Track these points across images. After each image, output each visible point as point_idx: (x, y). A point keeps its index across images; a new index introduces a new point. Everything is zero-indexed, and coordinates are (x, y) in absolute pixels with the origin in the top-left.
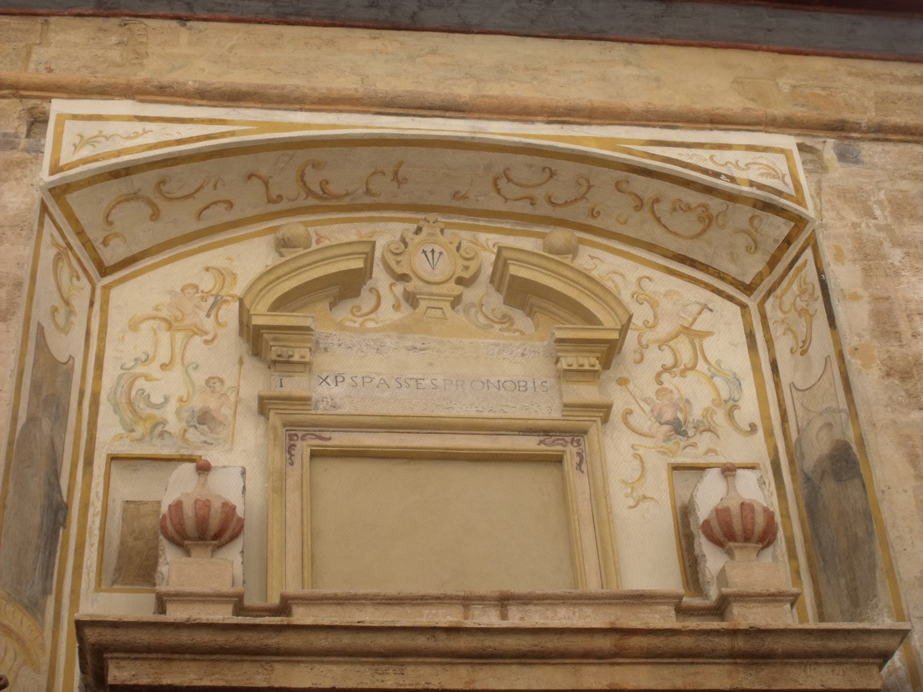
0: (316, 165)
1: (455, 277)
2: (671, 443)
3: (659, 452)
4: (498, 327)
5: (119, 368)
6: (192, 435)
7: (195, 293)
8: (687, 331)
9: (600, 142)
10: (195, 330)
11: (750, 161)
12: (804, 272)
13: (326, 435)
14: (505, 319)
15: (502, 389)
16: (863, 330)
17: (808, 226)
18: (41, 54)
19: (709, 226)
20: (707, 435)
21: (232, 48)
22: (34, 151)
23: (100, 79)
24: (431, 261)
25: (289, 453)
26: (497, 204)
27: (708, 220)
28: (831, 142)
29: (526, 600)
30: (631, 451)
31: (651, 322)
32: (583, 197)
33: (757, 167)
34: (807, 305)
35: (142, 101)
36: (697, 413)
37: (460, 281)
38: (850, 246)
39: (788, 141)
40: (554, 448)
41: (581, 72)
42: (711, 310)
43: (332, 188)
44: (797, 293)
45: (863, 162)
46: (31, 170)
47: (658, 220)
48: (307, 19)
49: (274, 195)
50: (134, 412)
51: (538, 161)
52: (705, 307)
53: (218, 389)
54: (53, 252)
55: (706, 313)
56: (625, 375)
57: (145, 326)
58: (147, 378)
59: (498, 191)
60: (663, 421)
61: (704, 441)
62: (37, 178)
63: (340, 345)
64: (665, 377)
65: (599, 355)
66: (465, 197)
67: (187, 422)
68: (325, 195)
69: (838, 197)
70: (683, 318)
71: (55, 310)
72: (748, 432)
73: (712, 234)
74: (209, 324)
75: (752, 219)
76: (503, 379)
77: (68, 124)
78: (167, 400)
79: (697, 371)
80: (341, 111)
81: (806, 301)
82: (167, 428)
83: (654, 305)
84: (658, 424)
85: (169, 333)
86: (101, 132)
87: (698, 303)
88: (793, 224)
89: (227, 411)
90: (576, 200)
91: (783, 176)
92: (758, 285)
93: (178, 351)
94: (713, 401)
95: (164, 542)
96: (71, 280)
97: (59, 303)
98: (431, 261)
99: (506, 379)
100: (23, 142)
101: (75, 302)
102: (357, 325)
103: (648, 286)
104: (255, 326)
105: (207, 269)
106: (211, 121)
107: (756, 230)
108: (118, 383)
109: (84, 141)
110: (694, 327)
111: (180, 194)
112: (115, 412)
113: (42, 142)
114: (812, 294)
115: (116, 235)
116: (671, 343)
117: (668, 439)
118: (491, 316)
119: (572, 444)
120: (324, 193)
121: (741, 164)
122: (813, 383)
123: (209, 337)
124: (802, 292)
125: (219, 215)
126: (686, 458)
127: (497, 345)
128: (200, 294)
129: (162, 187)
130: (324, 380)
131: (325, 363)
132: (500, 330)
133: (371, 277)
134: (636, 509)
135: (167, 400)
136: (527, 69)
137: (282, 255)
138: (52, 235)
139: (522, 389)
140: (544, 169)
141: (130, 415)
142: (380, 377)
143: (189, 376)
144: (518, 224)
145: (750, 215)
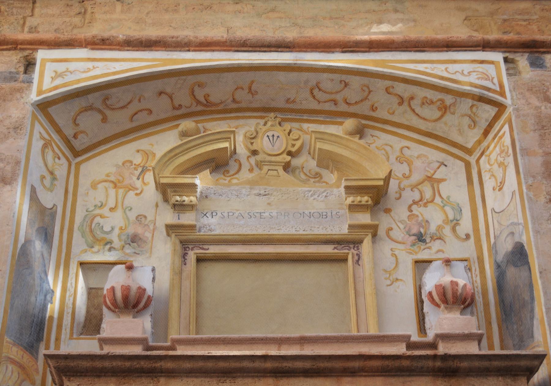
0: (201, 85)
1: (286, 151)
2: (415, 247)
3: (408, 252)
4: (312, 180)
5: (85, 211)
6: (128, 250)
7: (130, 166)
8: (429, 178)
10: (130, 187)
11: (472, 70)
12: (503, 139)
13: (206, 247)
14: (318, 176)
15: (312, 217)
16: (537, 173)
17: (507, 110)
19: (445, 112)
20: (438, 241)
21: (148, 13)
22: (28, 82)
23: (65, 36)
24: (272, 142)
25: (184, 258)
26: (314, 105)
27: (444, 109)
28: (526, 55)
30: (391, 252)
31: (407, 174)
32: (366, 98)
33: (475, 74)
34: (504, 160)
35: (93, 49)
36: (433, 228)
37: (290, 153)
38: (533, 121)
39: (498, 57)
40: (342, 251)
41: (366, 18)
42: (446, 166)
43: (212, 99)
44: (499, 152)
45: (546, 67)
46: (26, 94)
47: (413, 111)
49: (176, 104)
50: (94, 236)
52: (443, 164)
53: (143, 222)
54: (41, 143)
55: (443, 167)
56: (389, 207)
57: (100, 186)
58: (101, 216)
59: (314, 97)
60: (411, 233)
61: (436, 245)
62: (30, 99)
63: (215, 194)
64: (414, 207)
65: (371, 195)
66: (294, 102)
67: (125, 242)
68: (208, 104)
69: (528, 90)
70: (428, 171)
71: (43, 177)
72: (464, 239)
73: (448, 117)
74: (138, 184)
75: (472, 106)
76: (312, 211)
77: (48, 65)
78: (113, 229)
79: (435, 203)
81: (503, 157)
82: (113, 245)
83: (410, 164)
84: (408, 236)
85: (115, 190)
86: (68, 69)
87: (438, 162)
88: (497, 109)
89: (148, 235)
90: (362, 101)
91: (493, 78)
92: (475, 149)
93: (120, 200)
94: (444, 221)
95: (105, 310)
96: (54, 160)
98: (272, 142)
99: (315, 211)
100: (22, 76)
101: (57, 173)
102: (227, 182)
104: (162, 184)
105: (138, 151)
107: (474, 114)
108: (84, 220)
109: (58, 75)
110: (434, 177)
112: (83, 237)
113: (33, 77)
114: (507, 153)
115: (82, 132)
116: (419, 187)
117: (413, 245)
118: (308, 174)
119: (354, 249)
120: (207, 102)
121: (466, 72)
122: (505, 207)
123: (138, 192)
124: (502, 152)
125: (143, 118)
126: (423, 255)
127: (310, 191)
128: (134, 166)
129: (108, 103)
130: (205, 215)
132: (314, 182)
133: (236, 153)
134: (391, 286)
135: (113, 229)
136: (331, 18)
137: (182, 140)
138: (40, 133)
139: (324, 217)
141: (92, 239)
142: (238, 212)
143: (126, 214)
144: (327, 118)
145: (470, 105)
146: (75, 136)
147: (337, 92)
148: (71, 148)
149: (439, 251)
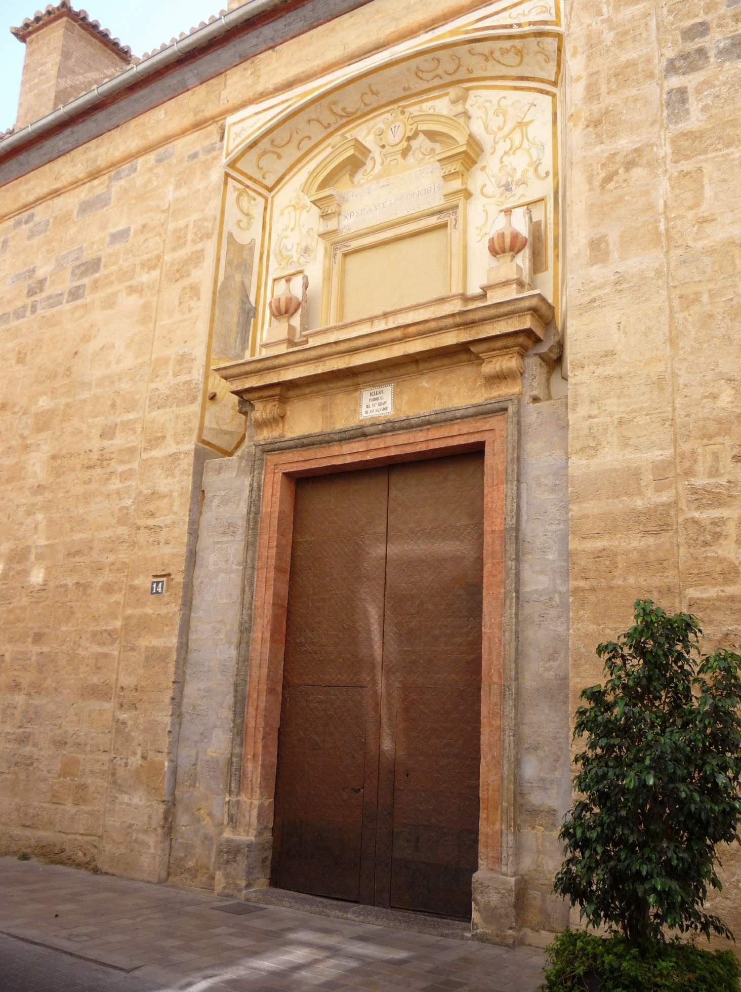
0: (335, 103)
9: (452, 33)
13: (349, 244)
18: (224, 94)
19: (522, 56)
26: (426, 86)
29: (395, 313)
36: (518, 175)
43: (349, 110)
47: (499, 62)
48: (321, 21)
51: (426, 56)
54: (236, 193)
58: (286, 237)
59: (421, 79)
64: (505, 158)
66: (409, 88)
73: (526, 60)
75: (538, 43)
76: (420, 190)
80: (333, 71)
90: (458, 68)
91: (550, 8)
97: (241, 216)
103: (504, 103)
106: (283, 102)
111: (283, 143)
115: (267, 172)
121: (526, 13)
123: (308, 209)
125: (307, 145)
131: (347, 208)
140: (433, 59)
146: (264, 177)
147: (437, 68)
148: (266, 188)
149: (523, 195)
